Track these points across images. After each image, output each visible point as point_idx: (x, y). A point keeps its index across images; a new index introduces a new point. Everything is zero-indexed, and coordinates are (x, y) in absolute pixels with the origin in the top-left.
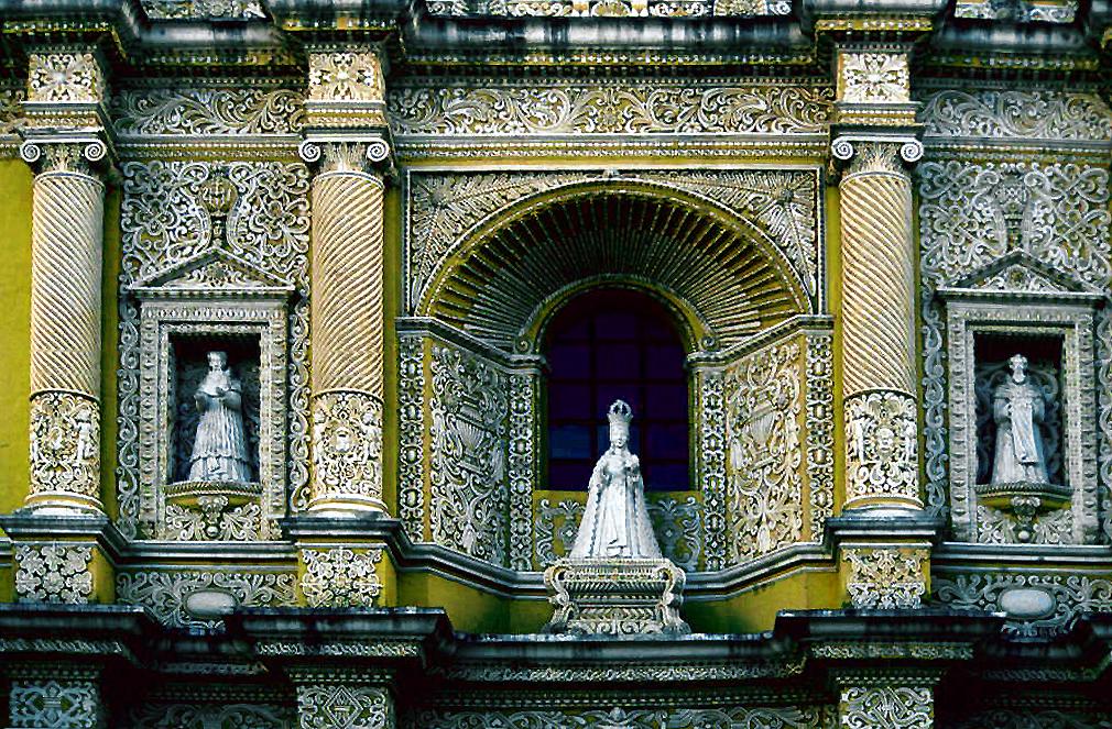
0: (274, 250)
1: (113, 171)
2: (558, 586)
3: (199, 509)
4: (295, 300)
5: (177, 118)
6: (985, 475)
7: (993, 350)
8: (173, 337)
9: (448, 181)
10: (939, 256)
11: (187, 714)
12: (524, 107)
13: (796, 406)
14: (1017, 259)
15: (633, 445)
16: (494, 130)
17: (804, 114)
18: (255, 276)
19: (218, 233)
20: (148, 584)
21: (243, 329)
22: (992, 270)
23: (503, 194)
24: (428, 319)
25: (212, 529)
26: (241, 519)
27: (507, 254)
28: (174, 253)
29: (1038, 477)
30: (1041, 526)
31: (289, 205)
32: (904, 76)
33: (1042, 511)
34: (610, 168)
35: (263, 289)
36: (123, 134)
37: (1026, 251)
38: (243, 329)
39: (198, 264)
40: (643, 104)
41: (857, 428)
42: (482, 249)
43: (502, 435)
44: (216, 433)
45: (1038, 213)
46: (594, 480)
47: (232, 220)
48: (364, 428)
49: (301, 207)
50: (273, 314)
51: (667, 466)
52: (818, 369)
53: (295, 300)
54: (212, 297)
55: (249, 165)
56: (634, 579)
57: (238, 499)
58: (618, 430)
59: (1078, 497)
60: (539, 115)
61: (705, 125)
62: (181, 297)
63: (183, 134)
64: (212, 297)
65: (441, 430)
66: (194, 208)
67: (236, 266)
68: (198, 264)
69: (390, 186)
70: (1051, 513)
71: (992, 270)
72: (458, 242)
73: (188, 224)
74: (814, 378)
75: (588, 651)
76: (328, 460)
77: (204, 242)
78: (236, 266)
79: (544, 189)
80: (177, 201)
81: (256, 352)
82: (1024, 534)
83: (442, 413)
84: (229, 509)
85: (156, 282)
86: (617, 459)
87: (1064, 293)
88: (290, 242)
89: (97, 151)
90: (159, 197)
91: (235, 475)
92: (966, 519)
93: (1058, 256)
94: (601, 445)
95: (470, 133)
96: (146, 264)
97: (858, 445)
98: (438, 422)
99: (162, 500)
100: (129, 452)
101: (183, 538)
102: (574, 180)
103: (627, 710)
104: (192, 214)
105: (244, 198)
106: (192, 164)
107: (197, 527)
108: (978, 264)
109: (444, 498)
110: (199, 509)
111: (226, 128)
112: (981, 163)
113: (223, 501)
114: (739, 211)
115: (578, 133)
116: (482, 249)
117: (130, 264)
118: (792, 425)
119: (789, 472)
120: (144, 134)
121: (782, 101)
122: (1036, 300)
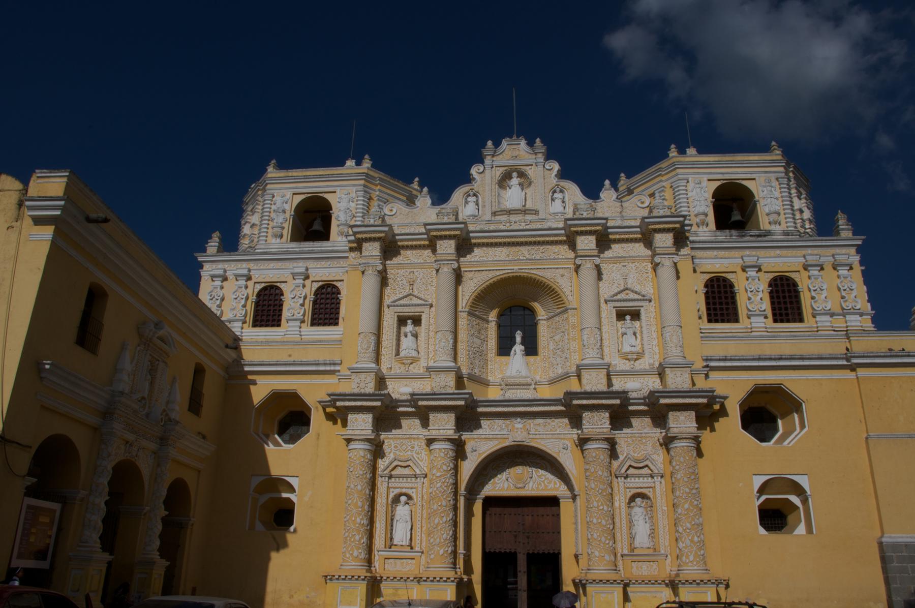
7: (621, 316)
8: (398, 316)
14: (627, 289)
15: (522, 343)
16: (485, 259)
18: (421, 299)
22: (620, 292)
32: (594, 241)
33: (636, 360)
35: (422, 302)
37: (629, 286)
39: (406, 297)
41: (585, 337)
44: (407, 343)
45: (632, 276)
46: (512, 352)
50: (426, 309)
53: (431, 306)
56: (523, 381)
57: (414, 360)
58: (518, 339)
66: (404, 282)
68: (406, 297)
71: (620, 292)
85: (394, 302)
86: (518, 348)
87: (640, 297)
89: (380, 267)
91: (414, 354)
93: (638, 288)
94: (515, 343)
97: (585, 343)
108: (616, 291)
118: (566, 337)
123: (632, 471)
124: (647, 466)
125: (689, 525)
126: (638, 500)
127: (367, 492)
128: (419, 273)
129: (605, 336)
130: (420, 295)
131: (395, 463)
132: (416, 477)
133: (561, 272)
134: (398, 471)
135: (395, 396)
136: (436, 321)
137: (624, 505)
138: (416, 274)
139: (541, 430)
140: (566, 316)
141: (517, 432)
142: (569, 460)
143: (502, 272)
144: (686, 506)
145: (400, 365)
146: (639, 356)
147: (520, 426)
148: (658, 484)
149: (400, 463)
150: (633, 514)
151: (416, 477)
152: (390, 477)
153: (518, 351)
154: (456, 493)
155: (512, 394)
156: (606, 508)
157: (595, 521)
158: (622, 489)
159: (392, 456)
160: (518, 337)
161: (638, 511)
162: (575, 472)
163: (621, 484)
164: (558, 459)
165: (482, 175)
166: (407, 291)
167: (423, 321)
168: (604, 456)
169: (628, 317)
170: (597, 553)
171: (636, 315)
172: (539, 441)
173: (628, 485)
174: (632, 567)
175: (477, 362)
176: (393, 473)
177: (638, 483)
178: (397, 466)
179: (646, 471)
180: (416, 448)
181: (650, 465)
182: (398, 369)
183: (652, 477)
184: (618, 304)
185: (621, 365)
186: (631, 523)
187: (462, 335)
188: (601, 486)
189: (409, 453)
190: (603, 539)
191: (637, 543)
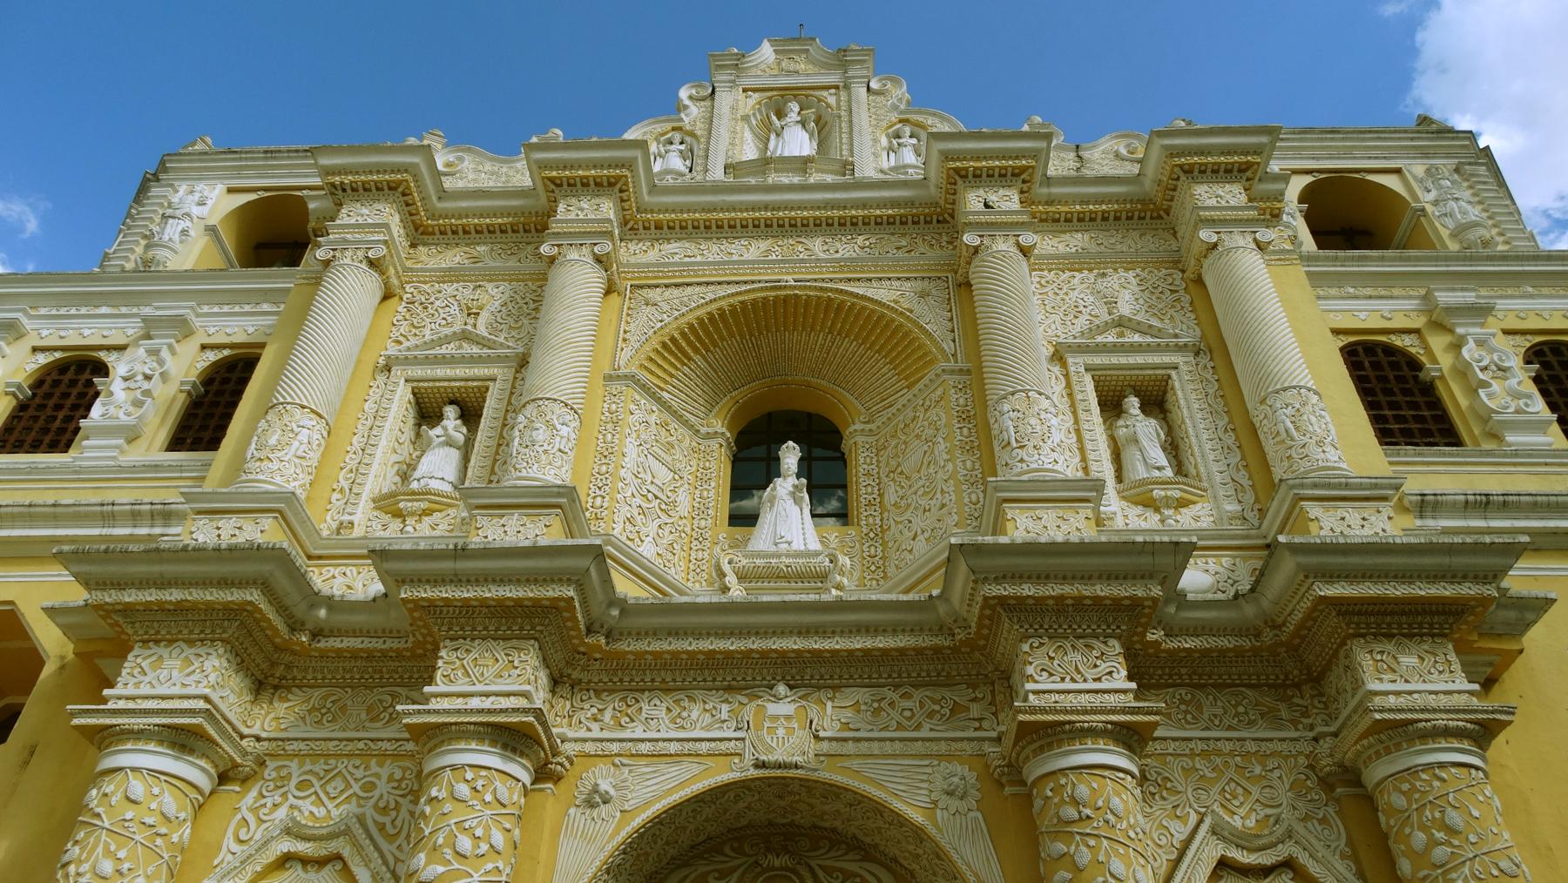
51: (828, 487)
103: (791, 687)
107: (396, 525)
112: (1080, 271)
131: (286, 845)
145: (387, 518)
147: (785, 708)
160: (790, 455)
165: (708, 103)
169: (1133, 403)
172: (855, 764)
175: (652, 528)
181: (1303, 858)
184: (1098, 360)
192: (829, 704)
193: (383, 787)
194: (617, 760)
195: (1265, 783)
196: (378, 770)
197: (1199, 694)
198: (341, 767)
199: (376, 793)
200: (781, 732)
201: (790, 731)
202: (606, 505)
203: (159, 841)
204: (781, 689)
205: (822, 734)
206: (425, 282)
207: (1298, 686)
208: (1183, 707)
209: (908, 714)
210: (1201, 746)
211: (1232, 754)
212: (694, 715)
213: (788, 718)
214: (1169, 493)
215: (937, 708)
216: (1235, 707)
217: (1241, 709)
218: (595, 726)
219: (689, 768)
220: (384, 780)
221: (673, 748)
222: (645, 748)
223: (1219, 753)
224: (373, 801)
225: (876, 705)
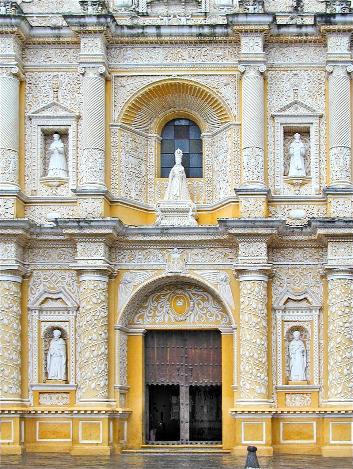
0: (73, 101)
1: (23, 76)
2: (158, 209)
3: (50, 186)
4: (79, 118)
5: (43, 58)
6: (286, 174)
8: (42, 130)
9: (126, 78)
10: (273, 103)
11: (46, 252)
12: (148, 54)
13: (230, 152)
17: (233, 56)
18: (66, 110)
19: (55, 96)
20: (34, 210)
21: (63, 127)
22: (289, 106)
23: (142, 82)
24: (119, 123)
25: (54, 192)
26: (63, 189)
27: (144, 102)
28: (42, 102)
29: (302, 173)
30: (303, 189)
31: (77, 87)
33: (302, 184)
34: (174, 74)
36: (26, 64)
38: (63, 127)
40: (185, 55)
42: (136, 101)
43: (142, 160)
47: (60, 92)
48: (98, 160)
49: (81, 87)
52: (236, 139)
54: (53, 117)
55: (65, 73)
57: (62, 183)
59: (314, 180)
60: (153, 57)
61: (203, 60)
62: (44, 117)
63: (45, 63)
64: (53, 117)
65: (122, 159)
67: (62, 107)
69: (107, 80)
70: (306, 185)
71: (289, 106)
72: (128, 99)
73: (46, 93)
74: (235, 142)
75: (164, 231)
76: (87, 170)
77: (51, 99)
78: (62, 107)
79: (154, 81)
80: (43, 86)
81: (67, 135)
82: (297, 192)
83: (124, 154)
84: (59, 186)
87: (311, 113)
88: (78, 99)
90: (38, 84)
92: (279, 187)
95: (133, 63)
96: (33, 106)
98: (123, 157)
99: (39, 183)
100: (29, 167)
101: (45, 195)
102: (164, 78)
104: (47, 90)
105: (64, 84)
106: (47, 73)
109: (125, 181)
110: (50, 186)
111: (58, 61)
113: (58, 183)
114: (213, 88)
115: (165, 62)
116: (136, 101)
117: (28, 106)
118: (229, 157)
119: (228, 172)
120: (33, 64)
121: (226, 52)
122: (301, 116)
123: (291, 304)
124: (306, 298)
125: (339, 359)
126: (296, 334)
127: (15, 326)
128: (65, 78)
129: (270, 157)
130: (66, 105)
131: (46, 296)
132: (67, 310)
133: (225, 80)
134: (50, 304)
135: (38, 222)
136: (86, 134)
137: (280, 339)
138: (61, 78)
139: (199, 260)
140: (229, 133)
141: (174, 264)
142: (224, 293)
143: (158, 79)
144: (339, 340)
145: (46, 188)
146: (304, 181)
147: (178, 256)
148: (316, 318)
149: (50, 296)
150: (291, 347)
151: (67, 310)
152: (41, 310)
153: (177, 172)
154: (109, 326)
155: (167, 222)
156: (258, 341)
157: (247, 354)
158: (279, 322)
159: (42, 288)
161: (296, 346)
162: (232, 305)
163: (279, 318)
164: (216, 290)
166: (51, 100)
167: (70, 136)
168: (260, 290)
170: (248, 386)
171: (305, 133)
173: (286, 318)
174: (286, 399)
176: (44, 306)
177: (295, 316)
178: (47, 298)
179: (304, 304)
180: (67, 279)
182: (44, 193)
183: (310, 310)
185: (284, 190)
186: (287, 358)
187: (114, 153)
188: (255, 320)
189: (60, 285)
190: (255, 371)
191: (293, 377)
192: (190, 254)
193: (67, 279)
194: (131, 271)
195: (306, 277)
196: (65, 274)
197: (295, 250)
198: (54, 273)
199: (66, 281)
200: (176, 263)
201: (178, 263)
202: (117, 183)
203: (16, 298)
204: (175, 250)
205: (187, 263)
206: (33, 72)
207: (322, 248)
208: (289, 255)
209: (212, 257)
210: (291, 266)
211: (299, 269)
212: (151, 257)
213: (178, 259)
214: (298, 181)
215: (220, 255)
216: (303, 254)
217: (305, 255)
218: (123, 260)
219: (152, 273)
220: (67, 276)
221: (146, 267)
222: (139, 267)
223: (296, 268)
224: (66, 283)
225: (203, 254)
